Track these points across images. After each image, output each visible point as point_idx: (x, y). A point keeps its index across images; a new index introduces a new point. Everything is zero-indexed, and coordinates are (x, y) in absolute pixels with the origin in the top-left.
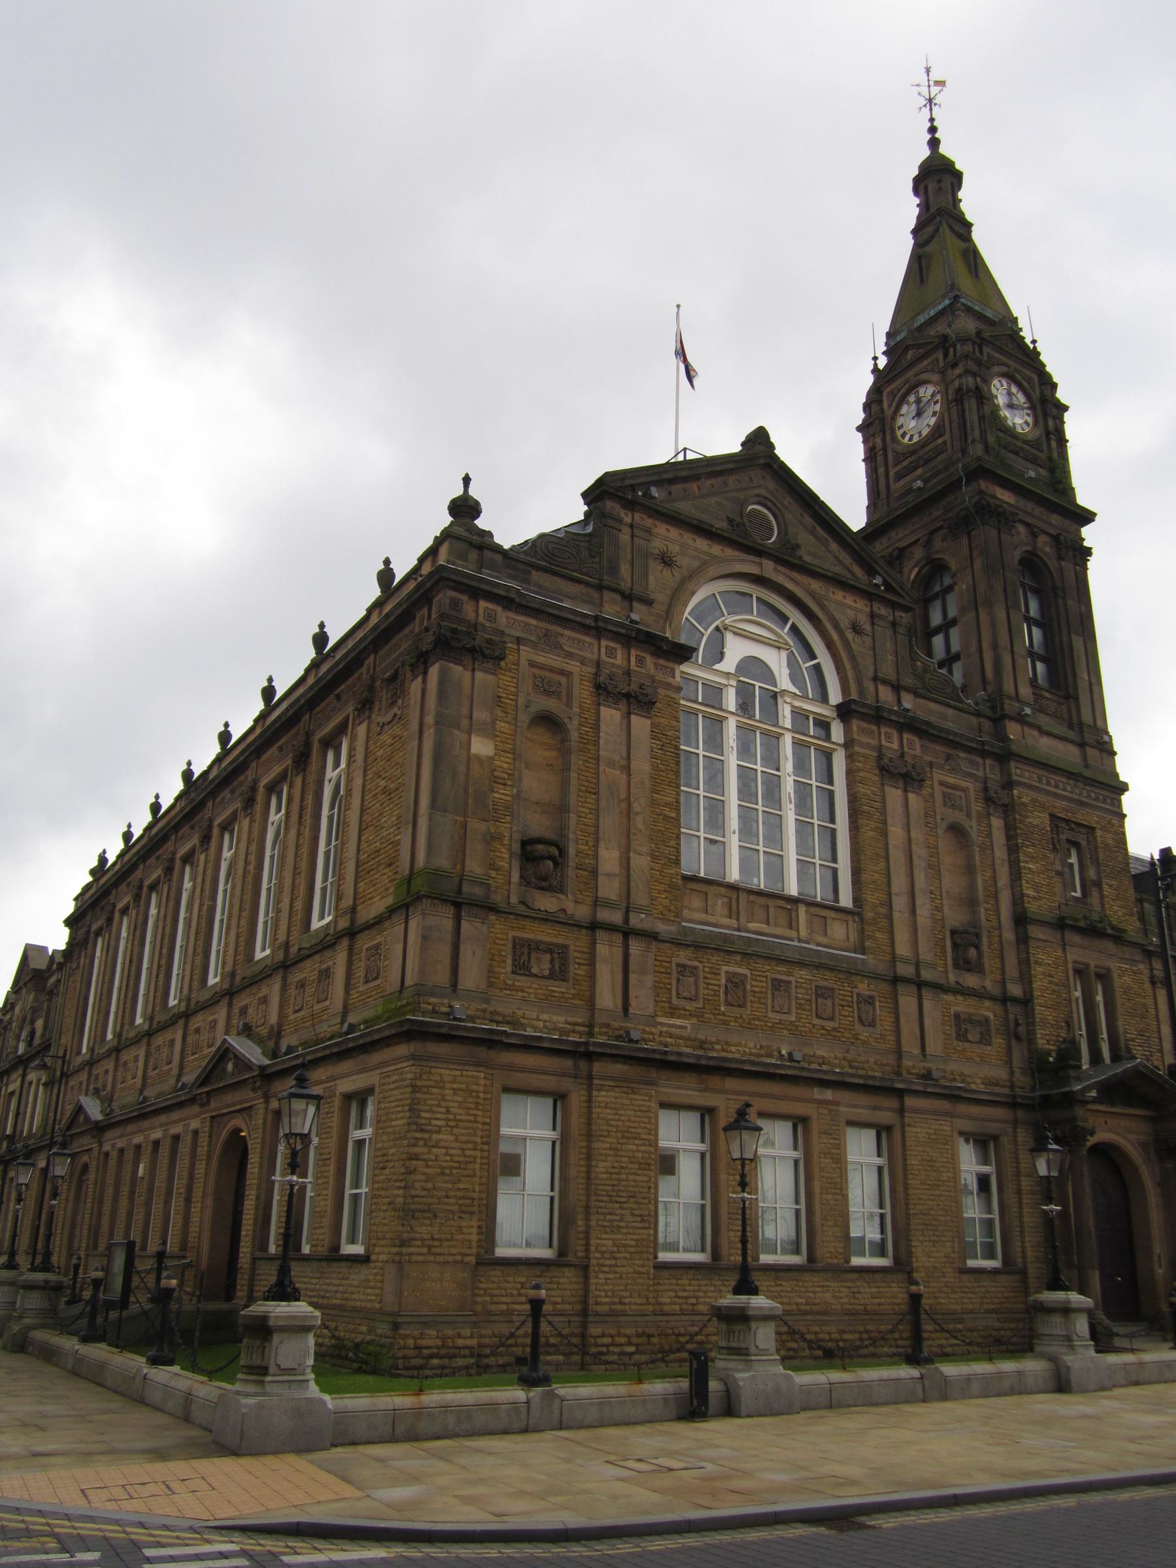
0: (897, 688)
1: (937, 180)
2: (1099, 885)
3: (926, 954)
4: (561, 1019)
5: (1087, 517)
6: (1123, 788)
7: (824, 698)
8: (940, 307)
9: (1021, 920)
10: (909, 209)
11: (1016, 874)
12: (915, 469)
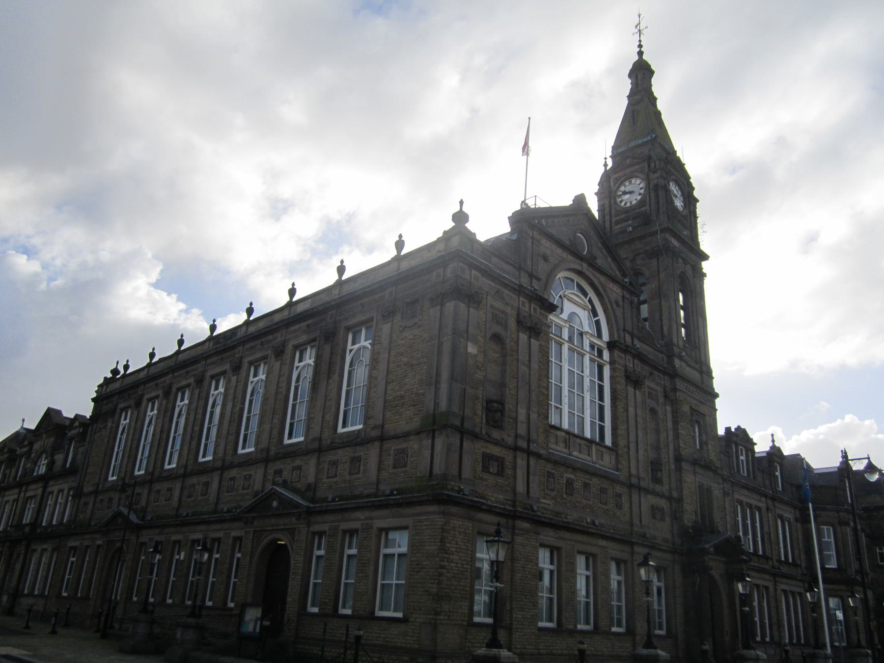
0: (633, 336)
1: (641, 73)
2: (706, 443)
3: (642, 475)
4: (501, 497)
5: (705, 257)
6: (716, 396)
7: (599, 336)
8: (645, 140)
9: (678, 459)
10: (627, 85)
11: (677, 436)
12: (627, 220)
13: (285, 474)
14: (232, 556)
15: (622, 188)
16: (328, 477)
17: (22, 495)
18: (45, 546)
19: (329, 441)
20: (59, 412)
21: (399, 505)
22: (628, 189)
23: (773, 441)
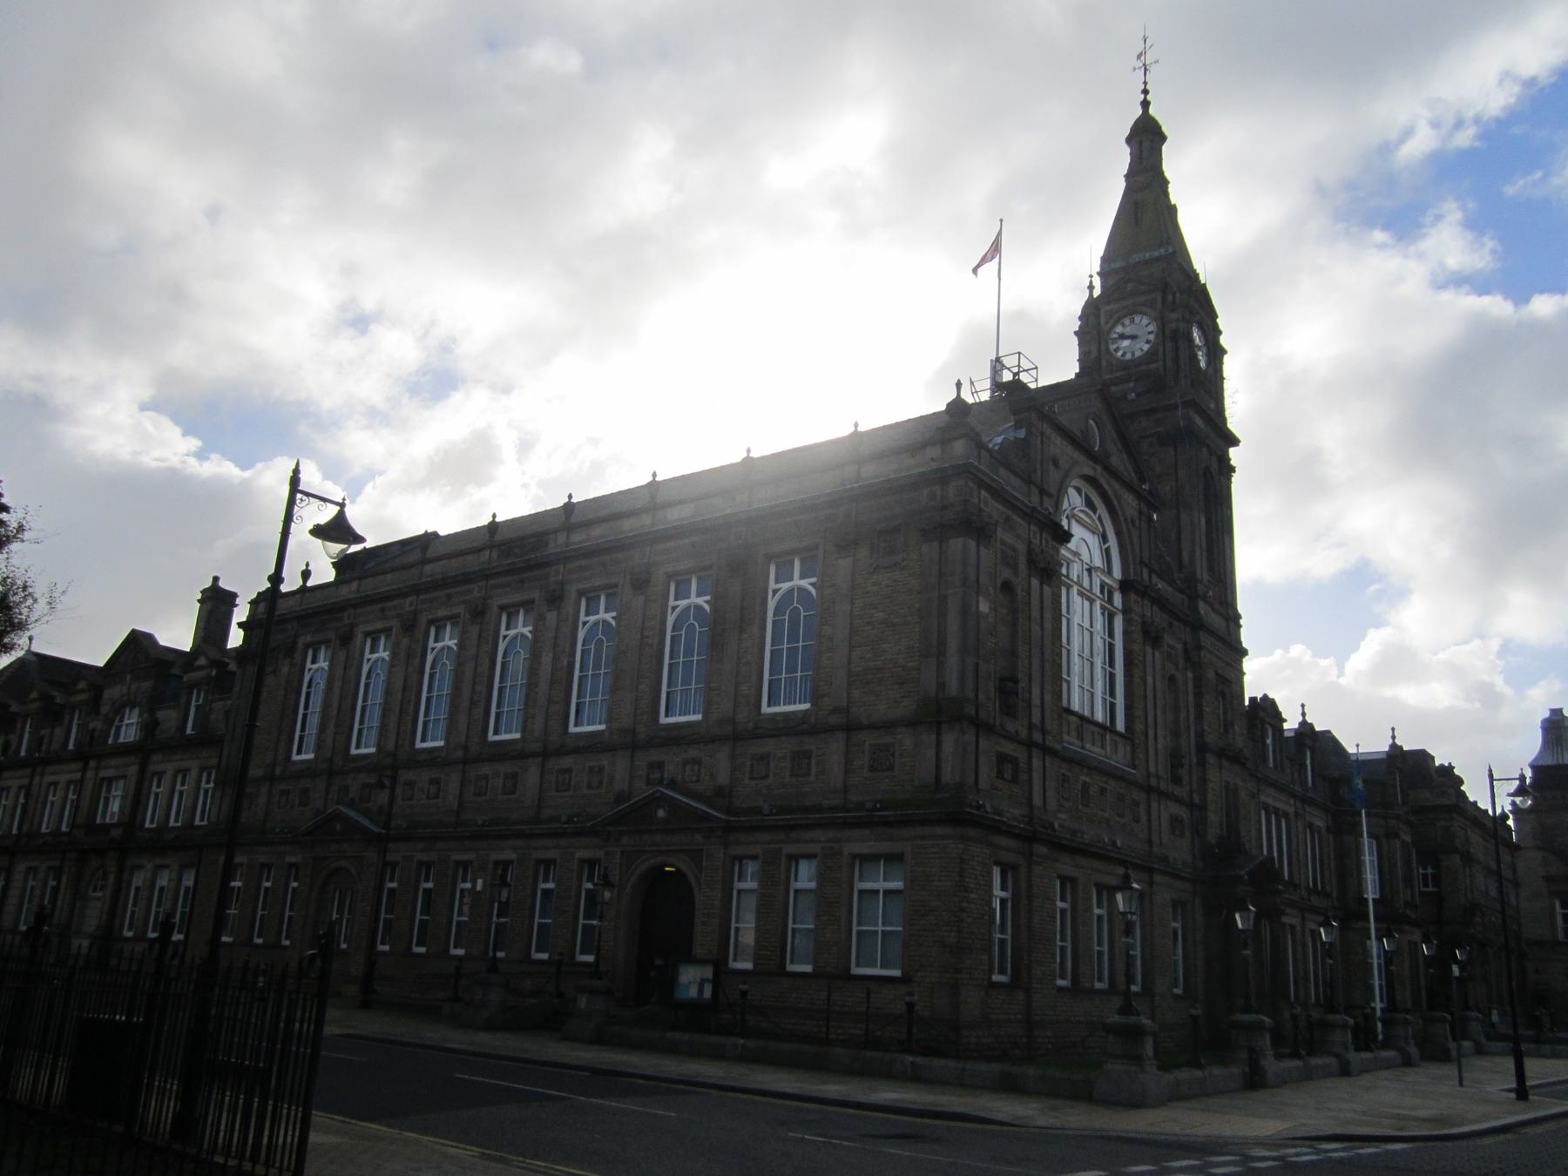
0: (1151, 571)
1: (1147, 138)
2: (1232, 724)
3: (1161, 773)
5: (1234, 441)
6: (1244, 653)
7: (1110, 572)
8: (1156, 254)
9: (1202, 748)
11: (1200, 716)
12: (1128, 381)
13: (670, 770)
14: (580, 886)
15: (1119, 329)
16: (752, 778)
17: (90, 774)
18: (159, 861)
19: (751, 725)
20: (150, 638)
21: (887, 823)
22: (1128, 331)
23: (1304, 714)
